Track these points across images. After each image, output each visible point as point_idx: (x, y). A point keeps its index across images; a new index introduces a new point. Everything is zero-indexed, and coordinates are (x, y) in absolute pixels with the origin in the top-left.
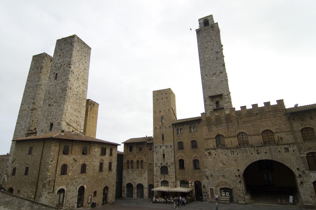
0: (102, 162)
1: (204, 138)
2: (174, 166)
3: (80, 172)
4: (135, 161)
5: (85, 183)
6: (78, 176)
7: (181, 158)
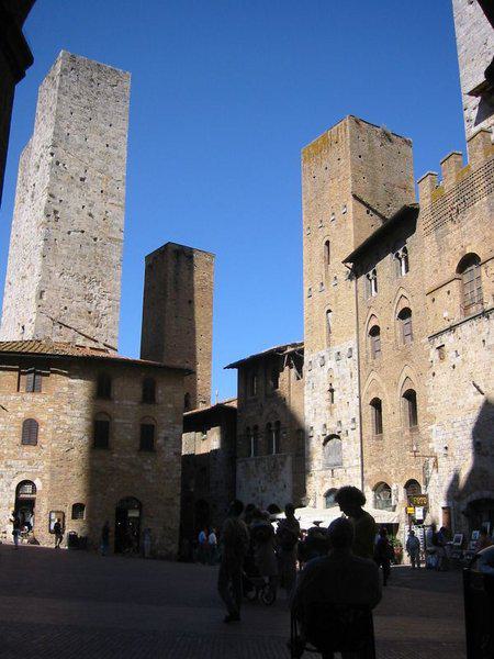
0: (103, 418)
1: (427, 289)
2: (358, 429)
3: (18, 440)
4: (262, 425)
5: (36, 473)
6: (12, 452)
7: (374, 395)
